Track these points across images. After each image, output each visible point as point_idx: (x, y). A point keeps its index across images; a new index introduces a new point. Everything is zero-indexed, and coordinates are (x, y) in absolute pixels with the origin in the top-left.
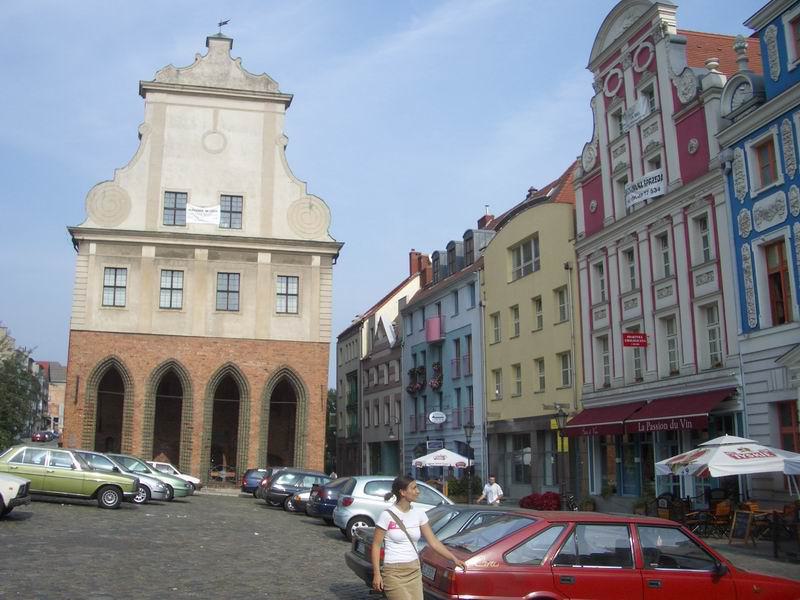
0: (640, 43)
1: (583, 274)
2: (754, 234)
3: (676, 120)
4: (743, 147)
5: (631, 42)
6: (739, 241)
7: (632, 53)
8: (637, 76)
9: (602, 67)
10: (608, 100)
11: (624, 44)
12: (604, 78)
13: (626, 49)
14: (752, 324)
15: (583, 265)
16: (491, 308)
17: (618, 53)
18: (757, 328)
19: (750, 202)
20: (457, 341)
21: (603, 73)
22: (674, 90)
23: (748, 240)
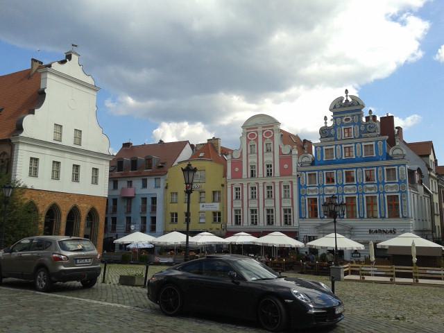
0: (268, 130)
1: (229, 190)
2: (306, 195)
5: (263, 127)
6: (300, 196)
7: (263, 131)
9: (247, 129)
10: (248, 141)
12: (248, 133)
15: (229, 186)
17: (257, 128)
18: (305, 218)
20: (144, 200)
21: (248, 131)
22: (280, 149)
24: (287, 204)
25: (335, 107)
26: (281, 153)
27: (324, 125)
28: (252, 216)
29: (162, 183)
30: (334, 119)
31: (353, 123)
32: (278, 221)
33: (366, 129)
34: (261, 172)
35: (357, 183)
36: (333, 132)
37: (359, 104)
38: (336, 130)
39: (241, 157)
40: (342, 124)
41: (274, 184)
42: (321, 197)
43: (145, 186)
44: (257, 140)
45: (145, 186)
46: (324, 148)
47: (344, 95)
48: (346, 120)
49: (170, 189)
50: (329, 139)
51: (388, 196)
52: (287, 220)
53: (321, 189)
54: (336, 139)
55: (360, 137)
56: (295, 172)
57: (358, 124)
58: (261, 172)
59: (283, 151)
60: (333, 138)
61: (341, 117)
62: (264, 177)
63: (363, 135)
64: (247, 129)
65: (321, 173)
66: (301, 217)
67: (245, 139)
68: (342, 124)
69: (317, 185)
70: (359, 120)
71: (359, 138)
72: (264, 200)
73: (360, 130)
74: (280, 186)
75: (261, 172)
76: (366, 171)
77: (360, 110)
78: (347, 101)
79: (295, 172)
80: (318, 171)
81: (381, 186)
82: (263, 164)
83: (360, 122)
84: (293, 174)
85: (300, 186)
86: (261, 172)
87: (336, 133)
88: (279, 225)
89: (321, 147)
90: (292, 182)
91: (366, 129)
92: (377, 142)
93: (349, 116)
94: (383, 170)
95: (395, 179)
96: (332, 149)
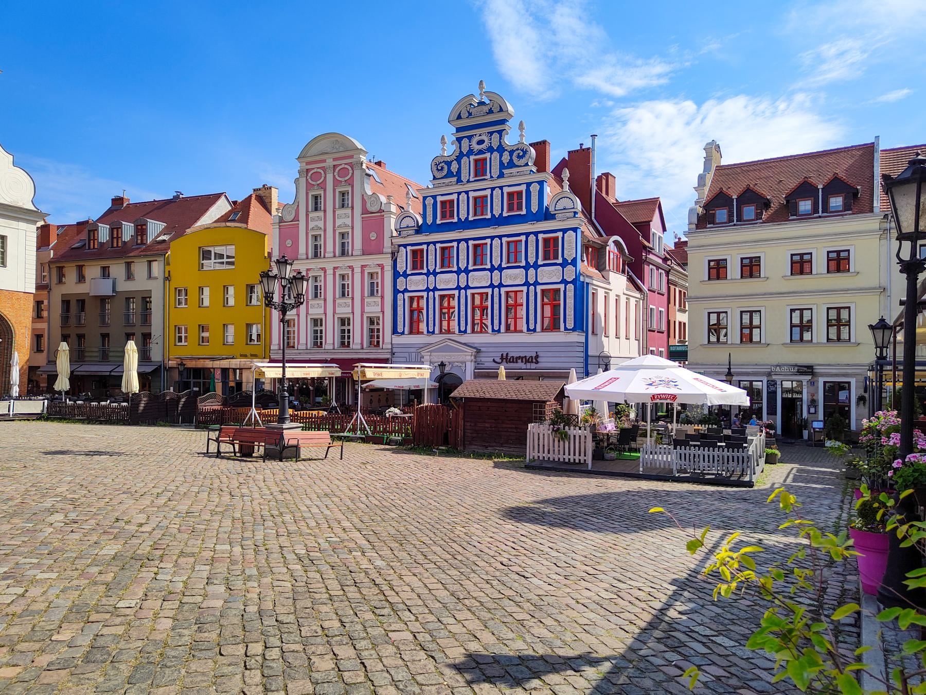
2: (406, 290)
3: (362, 218)
4: (406, 248)
5: (335, 159)
6: (396, 291)
8: (336, 183)
9: (308, 163)
10: (309, 187)
11: (330, 158)
12: (308, 170)
13: (330, 162)
14: (400, 329)
16: (176, 282)
17: (324, 161)
18: (403, 333)
19: (405, 275)
23: (403, 292)
24: (373, 309)
25: (459, 117)
26: (365, 211)
27: (438, 154)
28: (316, 332)
29: (157, 268)
30: (459, 140)
31: (490, 149)
32: (357, 339)
33: (511, 160)
34: (330, 248)
35: (492, 265)
36: (454, 167)
37: (501, 110)
38: (459, 164)
39: (296, 218)
40: (471, 152)
41: (353, 271)
42: (431, 293)
43: (129, 276)
44: (323, 186)
45: (129, 276)
46: (439, 199)
47: (476, 92)
48: (481, 142)
49: (176, 282)
50: (446, 181)
51: (543, 291)
52: (374, 338)
53: (431, 277)
54: (459, 181)
55: (501, 176)
56: (388, 248)
57: (497, 150)
58: (330, 248)
59: (368, 205)
60: (455, 179)
61: (470, 138)
62: (335, 256)
63: (505, 171)
64: (308, 163)
65: (431, 247)
66: (395, 331)
67: (303, 182)
68: (471, 152)
69: (425, 271)
70: (500, 142)
71: (499, 177)
72: (334, 301)
73: (501, 162)
74: (362, 272)
75: (330, 245)
76: (508, 243)
77: (503, 122)
78: (481, 103)
79: (388, 248)
80: (428, 244)
81: (532, 271)
82: (334, 231)
83: (501, 149)
84: (385, 250)
85: (396, 275)
86: (330, 245)
87: (459, 169)
88: (359, 347)
89: (434, 197)
90: (382, 267)
91: (511, 160)
92: (529, 185)
93: (483, 132)
94: (537, 241)
95: (557, 258)
96: (453, 201)
